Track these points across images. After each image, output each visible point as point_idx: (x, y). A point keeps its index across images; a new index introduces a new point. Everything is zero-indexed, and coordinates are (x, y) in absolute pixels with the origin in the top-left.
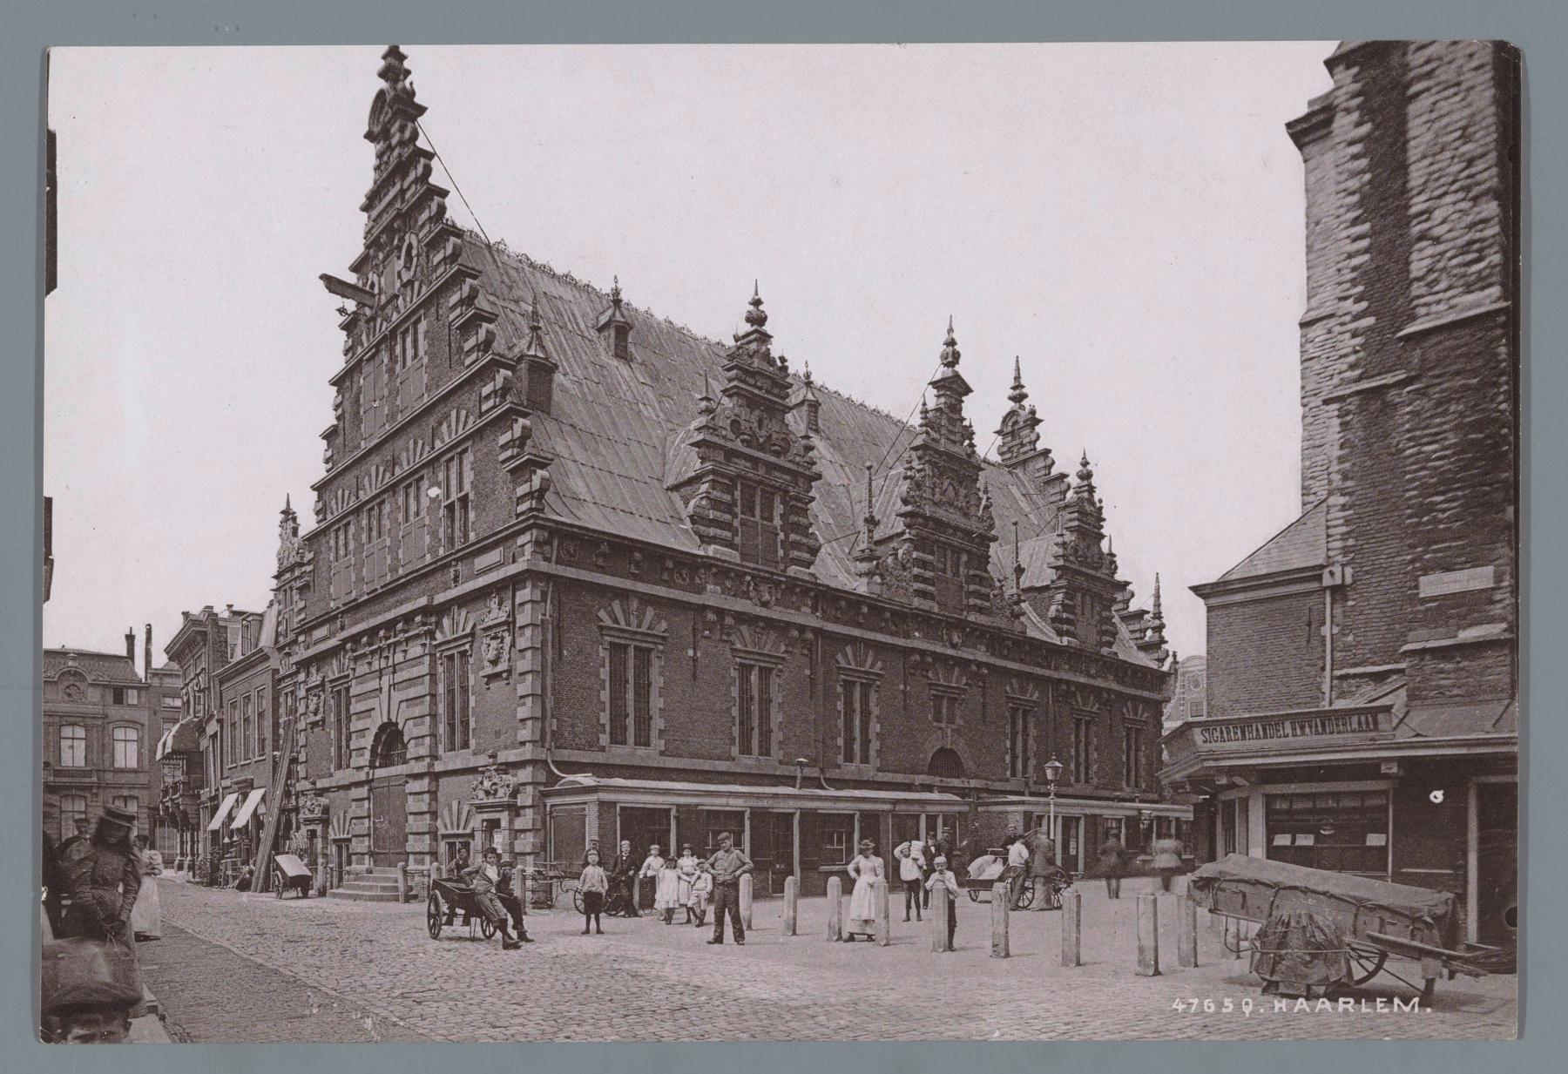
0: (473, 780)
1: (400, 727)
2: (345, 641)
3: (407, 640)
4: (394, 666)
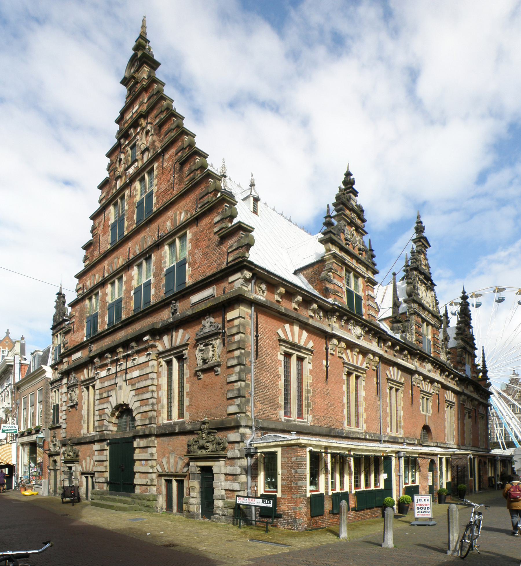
0: (184, 439)
1: (130, 407)
3: (138, 352)
4: (126, 369)
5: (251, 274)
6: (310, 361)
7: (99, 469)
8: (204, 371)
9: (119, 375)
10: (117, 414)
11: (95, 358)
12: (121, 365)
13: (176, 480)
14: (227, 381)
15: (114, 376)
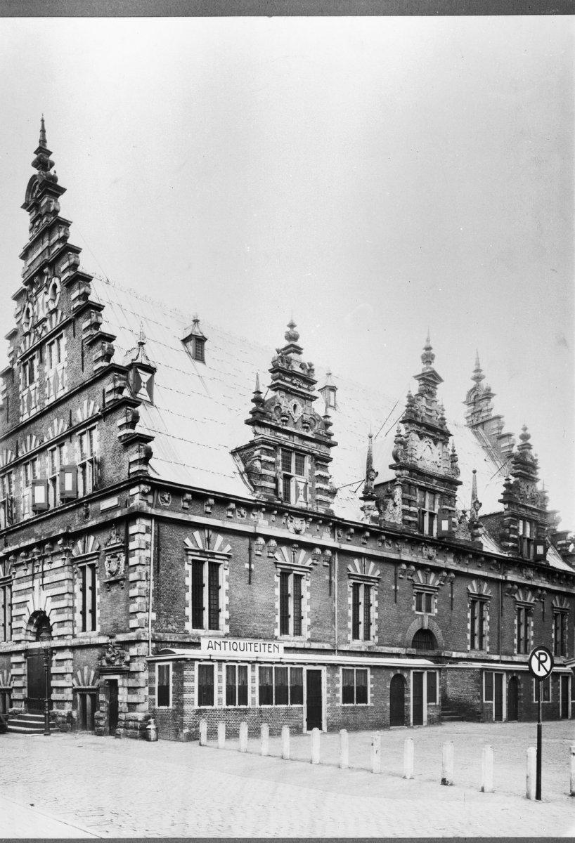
0: (96, 652)
1: (47, 615)
2: (9, 554)
3: (53, 555)
5: (150, 488)
6: (226, 568)
7: (18, 684)
8: (111, 583)
9: (36, 576)
10: (35, 621)
11: (11, 555)
12: (38, 566)
13: (90, 695)
14: (130, 596)
15: (31, 577)
